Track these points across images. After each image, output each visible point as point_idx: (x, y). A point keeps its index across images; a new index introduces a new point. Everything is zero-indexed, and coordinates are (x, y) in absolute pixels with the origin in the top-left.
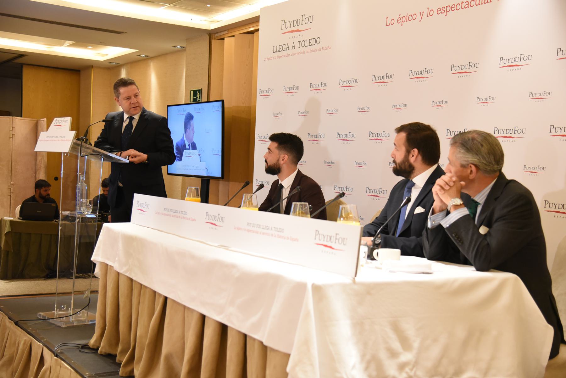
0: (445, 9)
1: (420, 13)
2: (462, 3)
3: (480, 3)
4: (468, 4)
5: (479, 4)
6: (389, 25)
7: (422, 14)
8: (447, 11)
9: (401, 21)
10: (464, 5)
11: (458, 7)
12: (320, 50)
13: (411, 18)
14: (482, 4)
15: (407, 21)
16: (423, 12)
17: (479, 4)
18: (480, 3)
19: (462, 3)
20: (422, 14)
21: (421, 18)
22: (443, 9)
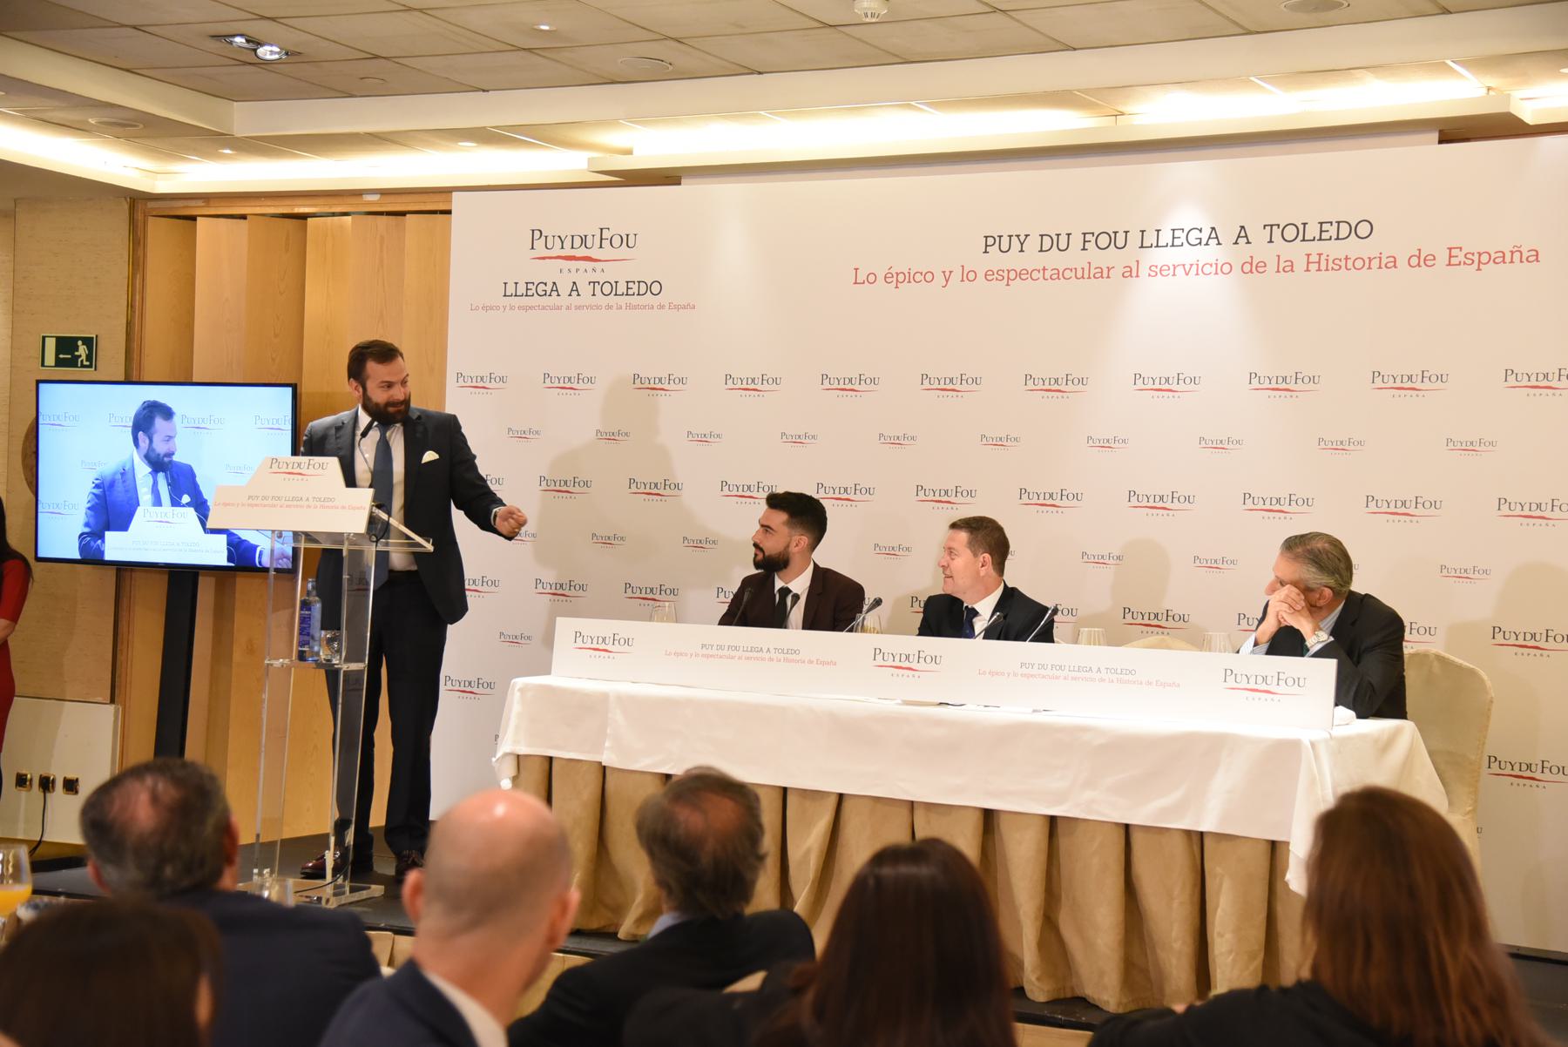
0: (1005, 274)
1: (944, 272)
2: (1044, 269)
3: (1086, 276)
4: (1058, 274)
5: (1083, 277)
6: (864, 283)
7: (947, 274)
8: (1008, 278)
9: (895, 279)
10: (1048, 274)
11: (1035, 275)
12: (661, 307)
13: (918, 277)
15: (909, 282)
16: (951, 272)
17: (1083, 277)
18: (1086, 276)
19: (1044, 269)
20: (947, 274)
21: (947, 281)
22: (1000, 273)
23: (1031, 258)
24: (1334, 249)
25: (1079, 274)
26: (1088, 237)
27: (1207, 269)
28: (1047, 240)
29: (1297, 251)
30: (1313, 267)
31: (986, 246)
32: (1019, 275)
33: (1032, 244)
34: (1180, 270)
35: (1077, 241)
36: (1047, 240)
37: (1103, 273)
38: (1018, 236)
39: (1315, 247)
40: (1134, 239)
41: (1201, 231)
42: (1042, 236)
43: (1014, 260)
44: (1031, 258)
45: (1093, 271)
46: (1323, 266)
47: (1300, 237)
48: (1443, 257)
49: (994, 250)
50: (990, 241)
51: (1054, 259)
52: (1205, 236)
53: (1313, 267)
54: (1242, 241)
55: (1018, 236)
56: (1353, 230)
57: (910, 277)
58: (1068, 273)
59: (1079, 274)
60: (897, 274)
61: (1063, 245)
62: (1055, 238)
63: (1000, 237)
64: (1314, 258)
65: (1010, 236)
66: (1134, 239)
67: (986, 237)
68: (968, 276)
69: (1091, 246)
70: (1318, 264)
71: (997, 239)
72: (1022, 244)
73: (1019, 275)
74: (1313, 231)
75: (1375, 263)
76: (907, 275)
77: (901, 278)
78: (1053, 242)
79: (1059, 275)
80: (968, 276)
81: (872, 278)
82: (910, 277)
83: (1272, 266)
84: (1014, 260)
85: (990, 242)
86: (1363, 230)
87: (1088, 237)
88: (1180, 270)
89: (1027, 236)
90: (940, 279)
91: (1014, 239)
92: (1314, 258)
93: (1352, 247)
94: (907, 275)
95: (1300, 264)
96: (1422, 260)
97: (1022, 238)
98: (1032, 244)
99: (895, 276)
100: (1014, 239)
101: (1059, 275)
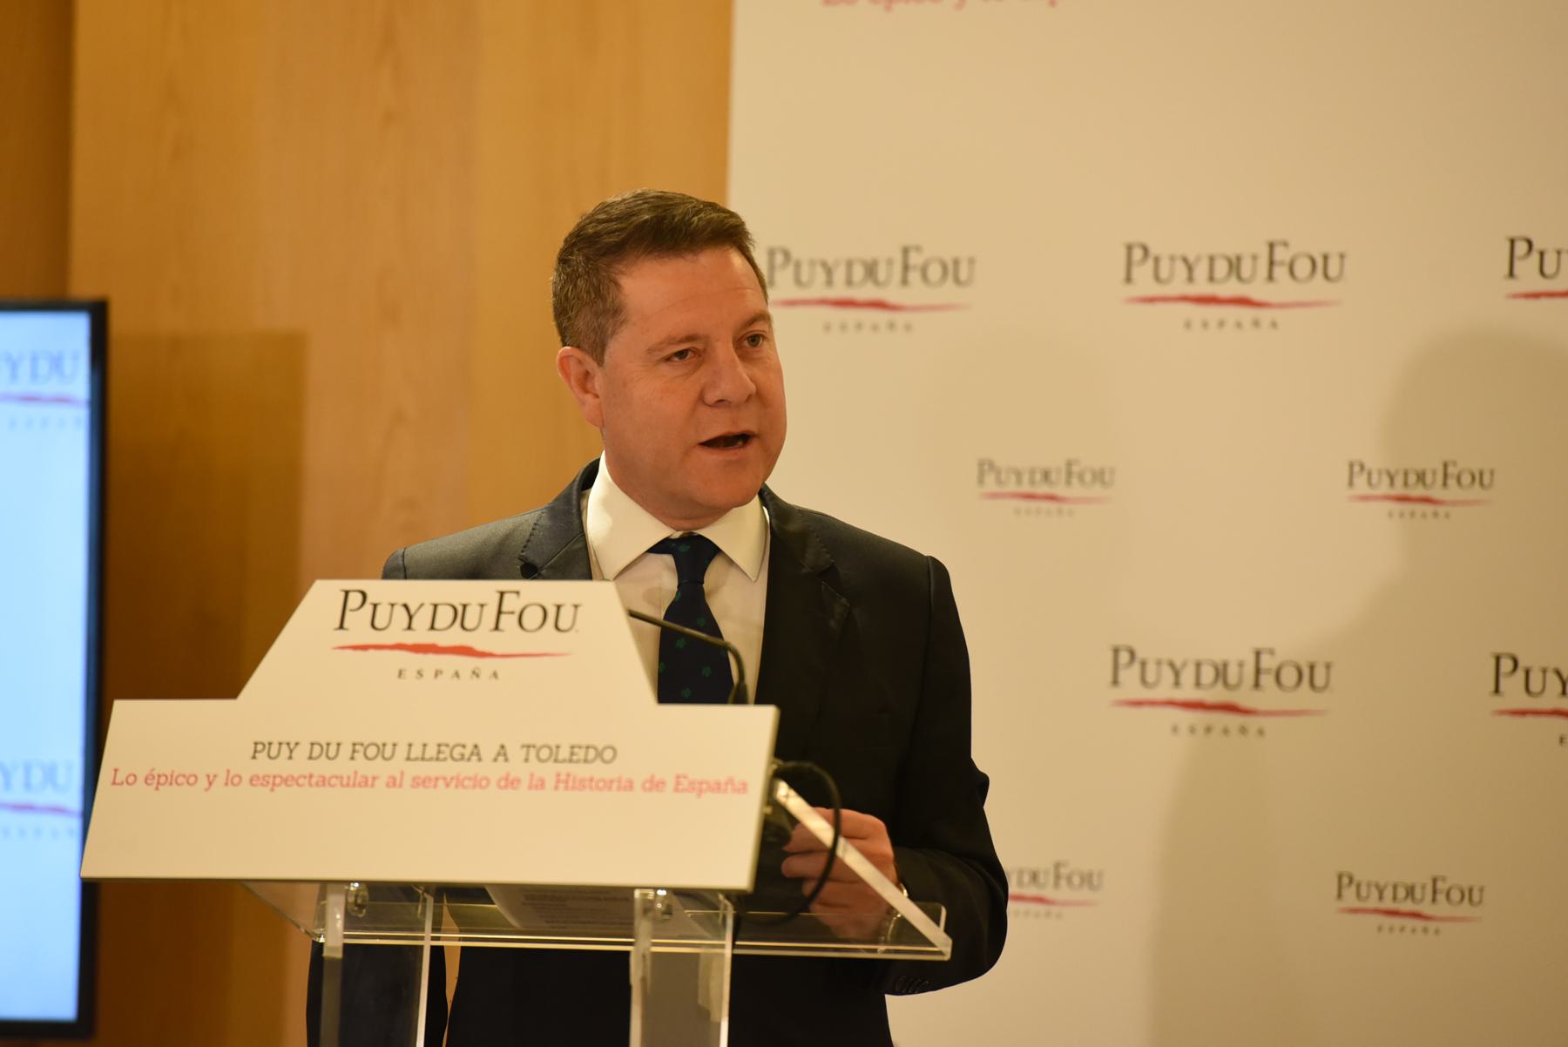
0: (271, 780)
2: (311, 776)
3: (351, 783)
9: (156, 781)
10: (314, 780)
11: (301, 781)
13: (181, 780)
14: (354, 785)
15: (171, 784)
18: (351, 783)
21: (210, 784)
22: (266, 778)
23: (300, 765)
24: (581, 771)
25: (345, 782)
26: (357, 747)
27: (467, 783)
28: (317, 750)
29: (548, 771)
30: (562, 786)
31: (255, 751)
32: (285, 781)
33: (302, 752)
34: (441, 783)
35: (346, 750)
36: (317, 750)
37: (367, 782)
38: (288, 744)
39: (564, 768)
40: (402, 751)
41: (464, 746)
42: (312, 744)
43: (282, 766)
44: (300, 765)
45: (358, 780)
46: (570, 784)
47: (553, 758)
48: (671, 784)
49: (262, 756)
50: (260, 747)
51: (322, 767)
52: (467, 752)
53: (562, 786)
54: (501, 758)
55: (288, 744)
56: (599, 754)
57: (172, 780)
58: (333, 781)
59: (345, 782)
60: (159, 776)
61: (332, 754)
62: (325, 747)
63: (270, 744)
64: (563, 777)
65: (280, 744)
66: (402, 751)
67: (256, 744)
68: (232, 780)
69: (359, 756)
70: (565, 782)
71: (267, 746)
72: (291, 751)
73: (285, 781)
74: (564, 753)
75: (615, 785)
76: (169, 778)
77: (163, 780)
78: (321, 750)
79: (324, 782)
80: (232, 780)
81: (131, 779)
82: (172, 780)
83: (525, 782)
84: (282, 766)
85: (258, 748)
86: (608, 754)
87: (357, 747)
88: (441, 783)
89: (297, 744)
90: (203, 782)
91: (284, 747)
92: (563, 777)
93: (597, 770)
94: (169, 778)
95: (550, 782)
96: (655, 785)
97: (292, 746)
98: (302, 752)
99: (156, 778)
100: (284, 747)
101: (324, 782)
